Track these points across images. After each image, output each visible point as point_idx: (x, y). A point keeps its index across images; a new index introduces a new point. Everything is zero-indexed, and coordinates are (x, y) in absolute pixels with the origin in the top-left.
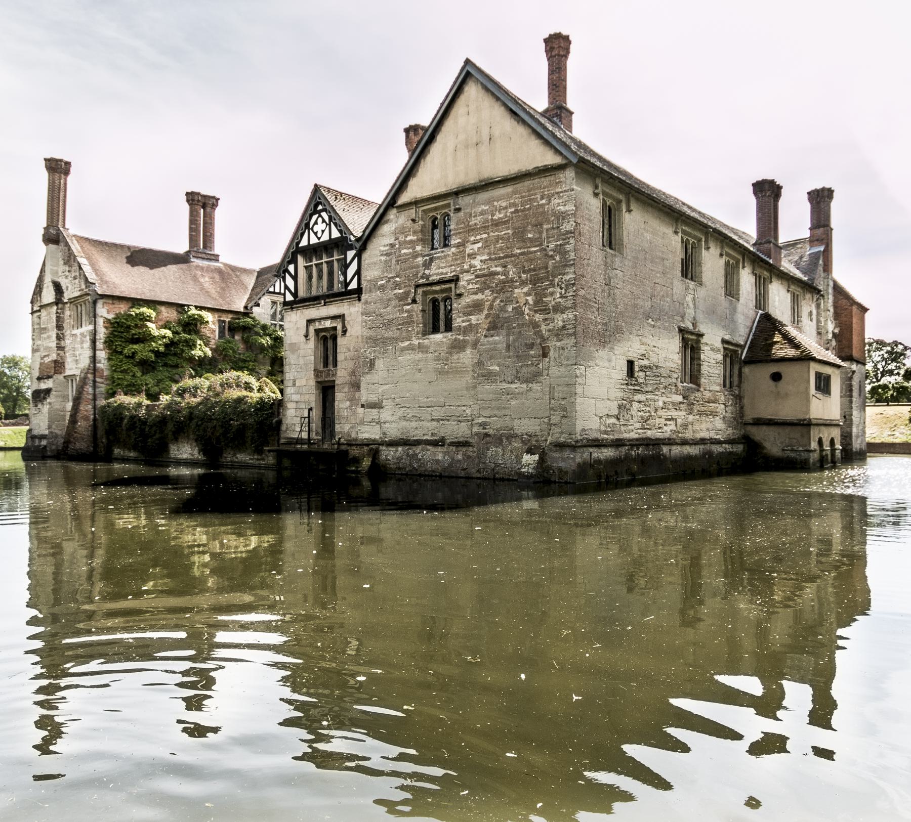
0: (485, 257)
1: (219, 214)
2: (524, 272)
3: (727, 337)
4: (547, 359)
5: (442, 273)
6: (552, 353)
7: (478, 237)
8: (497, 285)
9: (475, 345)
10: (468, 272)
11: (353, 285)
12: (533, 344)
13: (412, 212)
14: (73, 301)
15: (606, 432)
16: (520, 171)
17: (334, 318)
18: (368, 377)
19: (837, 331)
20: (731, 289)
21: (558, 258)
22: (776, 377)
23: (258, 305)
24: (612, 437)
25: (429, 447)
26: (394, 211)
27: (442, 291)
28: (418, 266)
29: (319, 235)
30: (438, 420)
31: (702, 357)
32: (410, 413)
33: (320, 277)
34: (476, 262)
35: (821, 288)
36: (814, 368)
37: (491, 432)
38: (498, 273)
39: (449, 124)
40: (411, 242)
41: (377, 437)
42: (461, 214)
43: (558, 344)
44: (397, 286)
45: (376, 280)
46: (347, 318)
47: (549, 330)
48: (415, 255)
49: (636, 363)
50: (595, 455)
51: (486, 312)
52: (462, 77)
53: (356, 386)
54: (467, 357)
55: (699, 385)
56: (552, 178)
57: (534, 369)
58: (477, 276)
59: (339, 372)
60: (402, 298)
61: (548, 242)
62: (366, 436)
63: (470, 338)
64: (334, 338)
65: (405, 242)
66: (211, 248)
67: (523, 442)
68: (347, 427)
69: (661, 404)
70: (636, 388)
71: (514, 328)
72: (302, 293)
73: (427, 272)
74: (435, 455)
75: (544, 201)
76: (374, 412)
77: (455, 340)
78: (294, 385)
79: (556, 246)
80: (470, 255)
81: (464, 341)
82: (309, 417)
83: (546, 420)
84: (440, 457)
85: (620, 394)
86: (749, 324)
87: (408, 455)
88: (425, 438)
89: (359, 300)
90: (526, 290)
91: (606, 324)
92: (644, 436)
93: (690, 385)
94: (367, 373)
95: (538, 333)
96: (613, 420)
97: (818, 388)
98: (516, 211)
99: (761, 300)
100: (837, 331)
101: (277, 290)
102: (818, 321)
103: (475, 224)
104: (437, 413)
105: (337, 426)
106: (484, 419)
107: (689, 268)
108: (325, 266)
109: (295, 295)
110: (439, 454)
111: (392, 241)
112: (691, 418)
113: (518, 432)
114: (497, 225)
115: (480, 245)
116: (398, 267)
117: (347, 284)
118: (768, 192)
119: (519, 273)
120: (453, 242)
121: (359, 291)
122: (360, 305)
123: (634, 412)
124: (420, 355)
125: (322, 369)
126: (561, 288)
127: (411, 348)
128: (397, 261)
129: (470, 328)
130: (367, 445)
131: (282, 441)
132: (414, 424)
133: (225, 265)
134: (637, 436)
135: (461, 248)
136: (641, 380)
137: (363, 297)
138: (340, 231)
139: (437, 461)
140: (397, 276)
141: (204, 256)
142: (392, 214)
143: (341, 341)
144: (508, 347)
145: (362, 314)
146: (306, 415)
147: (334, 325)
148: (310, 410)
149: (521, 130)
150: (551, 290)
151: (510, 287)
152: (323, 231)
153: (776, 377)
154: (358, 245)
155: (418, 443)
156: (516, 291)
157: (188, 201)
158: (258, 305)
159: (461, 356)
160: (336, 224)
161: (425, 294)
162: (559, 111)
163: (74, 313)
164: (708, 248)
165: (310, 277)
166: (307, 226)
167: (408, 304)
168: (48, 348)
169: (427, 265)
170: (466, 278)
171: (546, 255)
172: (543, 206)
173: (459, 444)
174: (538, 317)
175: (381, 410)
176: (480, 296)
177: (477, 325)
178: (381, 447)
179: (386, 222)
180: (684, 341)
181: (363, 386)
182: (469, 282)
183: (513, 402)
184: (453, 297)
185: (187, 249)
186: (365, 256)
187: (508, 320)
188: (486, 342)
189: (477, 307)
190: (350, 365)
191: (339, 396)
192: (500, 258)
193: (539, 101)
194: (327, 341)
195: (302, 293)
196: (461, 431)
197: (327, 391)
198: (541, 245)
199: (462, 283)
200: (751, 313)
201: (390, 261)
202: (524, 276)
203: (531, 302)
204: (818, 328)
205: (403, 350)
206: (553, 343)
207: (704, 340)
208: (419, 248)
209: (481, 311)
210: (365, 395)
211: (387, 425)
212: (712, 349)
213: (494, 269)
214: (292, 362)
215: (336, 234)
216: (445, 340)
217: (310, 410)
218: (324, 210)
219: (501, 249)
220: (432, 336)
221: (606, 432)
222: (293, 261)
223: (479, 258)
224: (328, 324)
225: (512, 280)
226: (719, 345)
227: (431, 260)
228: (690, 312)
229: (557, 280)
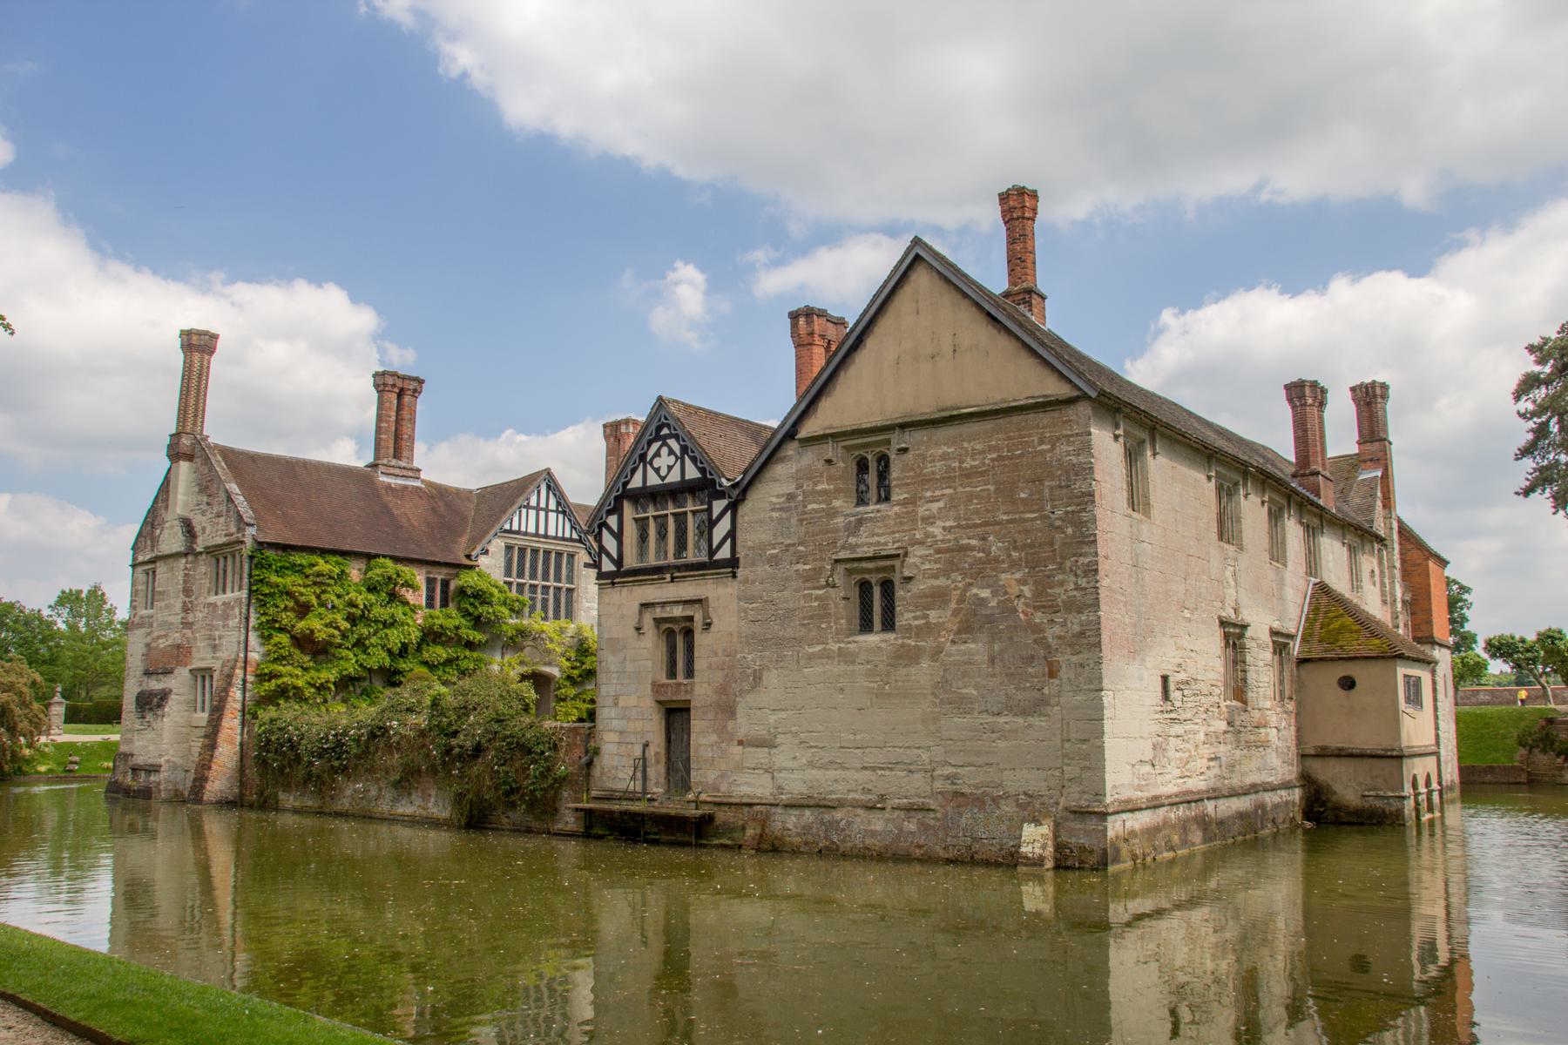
0: (948, 524)
1: (422, 405)
2: (1015, 548)
3: (1276, 625)
4: (1057, 681)
5: (878, 543)
6: (1063, 673)
7: (938, 493)
8: (971, 565)
9: (936, 653)
10: (922, 543)
11: (724, 553)
12: (1033, 657)
13: (829, 450)
14: (210, 551)
15: (1140, 788)
16: (1003, 401)
18: (750, 698)
19: (1407, 598)
20: (1277, 552)
21: (1070, 531)
22: (1348, 684)
23: (486, 552)
24: (1147, 794)
25: (860, 811)
26: (795, 445)
27: (878, 570)
28: (837, 531)
29: (663, 472)
30: (874, 769)
31: (1249, 659)
32: (826, 756)
33: (662, 535)
34: (936, 530)
35: (1382, 533)
36: (1402, 670)
37: (966, 790)
38: (972, 548)
39: (885, 325)
40: (825, 492)
41: (767, 793)
42: (909, 456)
43: (1074, 659)
44: (800, 558)
45: (762, 547)
46: (712, 604)
47: (1059, 637)
48: (834, 513)
49: (1171, 679)
50: (1129, 824)
51: (953, 605)
52: (908, 261)
53: (729, 710)
54: (923, 672)
55: (1245, 702)
56: (1056, 414)
57: (1036, 694)
58: (938, 551)
59: (697, 688)
60: (810, 578)
61: (1054, 507)
62: (745, 790)
63: (927, 644)
64: (689, 633)
65: (814, 492)
66: (410, 459)
67: (1019, 805)
68: (712, 776)
69: (1201, 737)
70: (1173, 715)
71: (1001, 631)
72: (630, 561)
73: (852, 540)
74: (869, 823)
75: (1044, 447)
77: (902, 646)
78: (616, 704)
79: (1067, 513)
80: (924, 519)
81: (918, 648)
82: (644, 759)
83: (1057, 773)
84: (878, 826)
85: (1156, 728)
86: (1299, 601)
87: (822, 823)
88: (851, 796)
89: (734, 576)
90: (1018, 575)
91: (1135, 625)
92: (1184, 788)
93: (1235, 703)
94: (748, 691)
95: (1041, 642)
96: (1148, 768)
97: (1408, 700)
98: (1000, 458)
99: (1312, 562)
100: (1407, 598)
101: (515, 527)
102: (1383, 584)
103: (933, 473)
104: (873, 757)
105: (693, 774)
106: (953, 770)
107: (1227, 528)
108: (671, 520)
109: (619, 562)
110: (878, 823)
111: (791, 488)
112: (1238, 752)
113: (1011, 791)
114: (968, 476)
115: (941, 504)
116: (803, 530)
117: (712, 552)
118: (1304, 397)
119: (1008, 549)
120: (894, 497)
122: (735, 583)
123: (1171, 753)
124: (843, 667)
125: (664, 680)
126: (1076, 575)
127: (826, 655)
128: (801, 521)
129: (928, 629)
130: (750, 805)
131: (594, 793)
132: (832, 774)
133: (429, 484)
134: (1175, 790)
135: (910, 508)
136: (1178, 704)
137: (740, 572)
138: (702, 470)
139: (873, 834)
140: (800, 544)
141: (397, 471)
142: (791, 449)
143: (701, 640)
144: (992, 661)
145: (740, 599)
146: (638, 752)
147: (689, 613)
148: (646, 745)
149: (1003, 341)
150: (1060, 577)
151: (993, 569)
152: (670, 468)
153: (1348, 684)
154: (735, 493)
155: (840, 804)
156: (1003, 576)
157: (376, 386)
158: (486, 552)
159: (913, 670)
160: (694, 460)
161: (849, 572)
162: (1025, 295)
163: (211, 570)
164: (1246, 496)
165: (643, 538)
166: (643, 457)
167: (819, 588)
168: (168, 625)
170: (918, 553)
171: (1052, 525)
172: (1043, 453)
173: (909, 809)
174: (1039, 618)
175: (774, 751)
176: (942, 582)
177: (940, 626)
178: (773, 810)
179: (783, 459)
180: (1226, 636)
181: (740, 711)
182: (924, 558)
183: (1001, 744)
184: (897, 583)
185: (370, 459)
186: (743, 509)
187: (990, 619)
188: (956, 652)
189: (938, 597)
190: (719, 677)
191: (696, 724)
192: (976, 526)
193: (996, 281)
194: (679, 636)
195: (630, 561)
196: (915, 786)
198: (1042, 509)
199: (911, 560)
200: (1301, 583)
201: (788, 519)
202: (1015, 554)
203: (1028, 594)
204: (1383, 594)
205: (811, 657)
206: (1064, 658)
207: (1249, 633)
208: (837, 503)
209: (947, 602)
210: (743, 725)
211: (784, 774)
212: (1259, 646)
213: (965, 541)
214: (613, 667)
215: (692, 473)
216: (883, 645)
217: (646, 745)
218: (670, 436)
219: (977, 512)
220: (861, 638)
221: (1140, 788)
222: (617, 509)
223: (939, 523)
224: (678, 611)
225: (996, 560)
226: (1266, 638)
227: (860, 522)
228: (1231, 592)
229: (1068, 564)
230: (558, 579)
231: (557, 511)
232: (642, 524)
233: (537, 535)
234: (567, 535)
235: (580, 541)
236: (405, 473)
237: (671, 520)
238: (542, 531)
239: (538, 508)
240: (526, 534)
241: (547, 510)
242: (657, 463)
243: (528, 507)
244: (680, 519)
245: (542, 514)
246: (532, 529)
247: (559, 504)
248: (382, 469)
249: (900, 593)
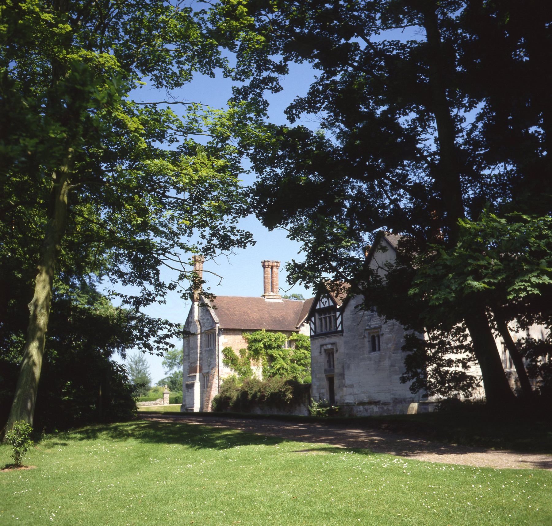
17: (333, 344)
27: (376, 332)
64: (333, 353)
76: (350, 390)
108: (328, 318)
109: (315, 332)
117: (337, 328)
121: (342, 331)
137: (344, 334)
161: (369, 334)
169: (369, 320)
186: (345, 314)
195: (318, 331)
197: (331, 381)
215: (331, 304)
220: (372, 353)
224: (329, 347)
232: (321, 319)
237: (328, 318)
242: (323, 300)
244: (330, 317)
248: (266, 297)
249: (381, 339)
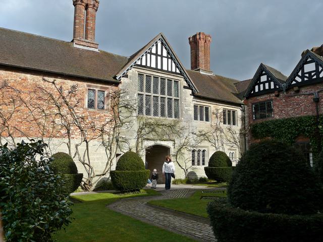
101: (144, 64)
133: (101, 51)
158: (126, 76)
230: (170, 94)
231: (167, 57)
233: (156, 69)
234: (174, 70)
235: (181, 74)
236: (89, 45)
238: (159, 67)
239: (156, 55)
240: (150, 68)
241: (162, 56)
243: (151, 54)
245: (159, 58)
246: (153, 66)
247: (168, 53)
